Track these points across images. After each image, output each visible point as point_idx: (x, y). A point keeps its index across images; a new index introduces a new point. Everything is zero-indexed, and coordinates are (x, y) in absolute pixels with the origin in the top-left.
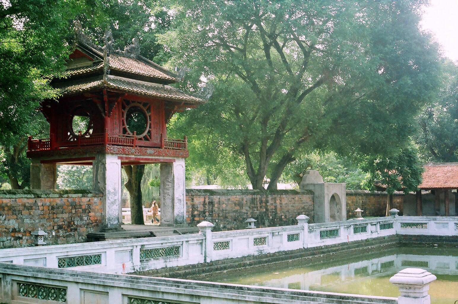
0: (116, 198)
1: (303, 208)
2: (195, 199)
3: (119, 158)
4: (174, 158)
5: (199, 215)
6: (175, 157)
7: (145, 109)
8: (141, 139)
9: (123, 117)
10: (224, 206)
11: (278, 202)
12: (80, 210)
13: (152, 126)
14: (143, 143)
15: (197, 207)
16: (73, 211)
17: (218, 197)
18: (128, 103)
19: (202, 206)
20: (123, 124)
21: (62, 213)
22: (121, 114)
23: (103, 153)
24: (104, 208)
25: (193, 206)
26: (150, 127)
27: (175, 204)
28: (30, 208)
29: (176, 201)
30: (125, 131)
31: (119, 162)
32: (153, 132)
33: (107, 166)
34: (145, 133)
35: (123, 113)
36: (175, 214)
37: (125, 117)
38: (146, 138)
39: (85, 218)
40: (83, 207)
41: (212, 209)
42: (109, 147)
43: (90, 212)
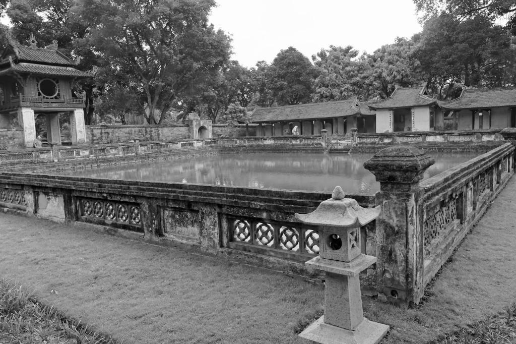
0: (32, 131)
1: (181, 134)
3: (32, 109)
5: (98, 140)
7: (54, 82)
8: (52, 98)
10: (117, 134)
11: (160, 132)
14: (54, 100)
20: (38, 90)
22: (36, 85)
23: (20, 107)
24: (23, 137)
25: (93, 135)
26: (59, 91)
27: (77, 134)
29: (78, 132)
30: (39, 94)
31: (33, 111)
32: (62, 94)
33: (23, 114)
34: (56, 95)
36: (78, 140)
37: (39, 86)
38: (56, 98)
39: (12, 142)
40: (9, 136)
42: (22, 104)
43: (14, 139)
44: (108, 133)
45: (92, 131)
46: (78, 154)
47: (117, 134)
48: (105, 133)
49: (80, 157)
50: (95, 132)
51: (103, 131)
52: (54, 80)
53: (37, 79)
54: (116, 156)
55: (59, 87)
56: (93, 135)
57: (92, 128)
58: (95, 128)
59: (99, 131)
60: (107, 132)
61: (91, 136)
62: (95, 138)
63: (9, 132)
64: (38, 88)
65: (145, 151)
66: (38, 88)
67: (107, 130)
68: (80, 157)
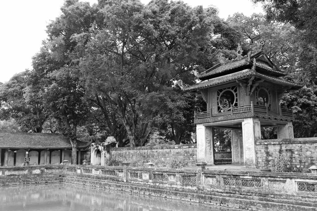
2: (270, 147)
4: (243, 119)
6: (244, 118)
7: (233, 91)
9: (218, 100)
12: (189, 154)
13: (238, 100)
15: (272, 154)
16: (186, 155)
17: (300, 145)
18: (221, 91)
19: (278, 153)
20: (218, 104)
21: (181, 155)
25: (268, 153)
26: (237, 101)
28: (168, 153)
31: (204, 127)
35: (218, 98)
39: (191, 159)
40: (190, 153)
41: (292, 155)
43: (193, 155)
44: (291, 151)
45: (267, 148)
46: (141, 177)
47: (308, 153)
48: (287, 150)
49: (141, 180)
50: (271, 149)
51: (284, 148)
52: (232, 89)
53: (218, 92)
54: (173, 186)
55: (237, 96)
56: (268, 153)
57: (266, 143)
58: (271, 144)
59: (278, 148)
60: (290, 150)
61: (265, 155)
62: (270, 158)
63: (190, 149)
64: (218, 102)
65: (212, 186)
66: (218, 102)
67: (290, 147)
68: (141, 180)
